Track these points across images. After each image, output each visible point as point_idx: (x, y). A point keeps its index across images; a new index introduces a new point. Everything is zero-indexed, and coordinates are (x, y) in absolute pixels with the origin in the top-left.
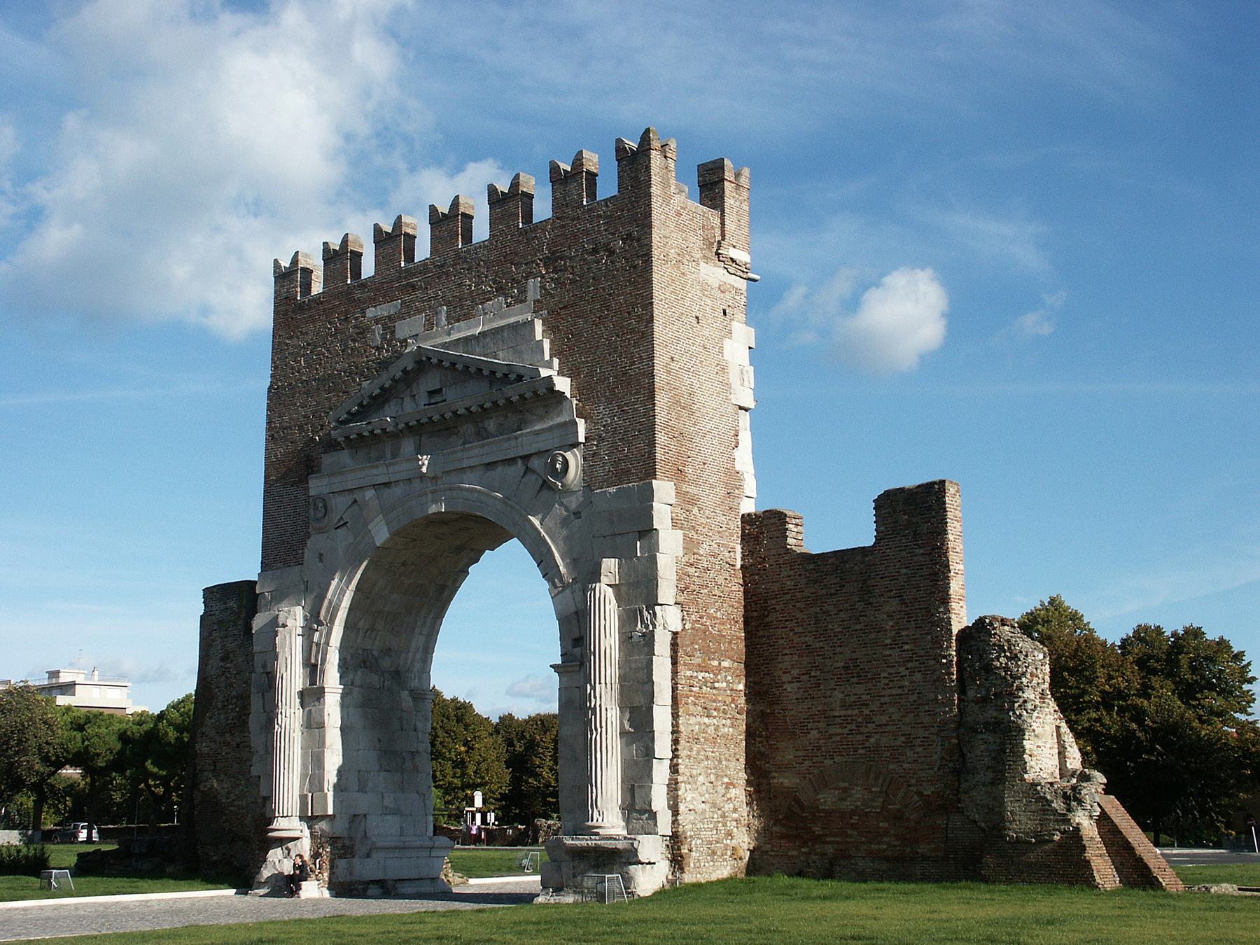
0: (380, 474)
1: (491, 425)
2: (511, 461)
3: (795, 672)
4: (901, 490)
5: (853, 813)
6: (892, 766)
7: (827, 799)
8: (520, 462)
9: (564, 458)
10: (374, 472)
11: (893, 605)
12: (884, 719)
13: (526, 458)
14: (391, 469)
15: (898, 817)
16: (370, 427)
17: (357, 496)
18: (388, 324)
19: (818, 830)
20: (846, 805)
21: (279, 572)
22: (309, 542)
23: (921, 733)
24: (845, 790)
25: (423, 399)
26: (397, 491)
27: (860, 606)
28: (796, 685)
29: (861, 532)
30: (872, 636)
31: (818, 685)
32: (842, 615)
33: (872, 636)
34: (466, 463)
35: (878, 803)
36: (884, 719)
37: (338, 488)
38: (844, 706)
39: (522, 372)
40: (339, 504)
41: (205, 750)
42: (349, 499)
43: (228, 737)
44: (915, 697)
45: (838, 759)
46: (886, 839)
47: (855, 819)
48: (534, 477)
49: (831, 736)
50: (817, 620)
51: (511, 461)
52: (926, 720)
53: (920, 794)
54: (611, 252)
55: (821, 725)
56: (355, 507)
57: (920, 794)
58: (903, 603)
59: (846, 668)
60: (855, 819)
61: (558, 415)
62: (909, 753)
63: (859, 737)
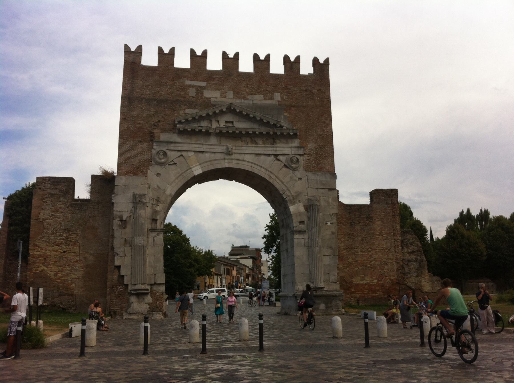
0: (197, 147)
1: (260, 141)
2: (269, 155)
3: (343, 240)
4: (382, 190)
5: (366, 284)
6: (380, 271)
7: (356, 280)
8: (273, 156)
9: (297, 159)
10: (197, 146)
11: (380, 222)
12: (376, 256)
13: (276, 155)
14: (205, 146)
15: (383, 286)
16: (200, 128)
17: (184, 154)
18: (200, 90)
19: (353, 290)
20: (364, 282)
21: (131, 178)
22: (150, 167)
23: (390, 261)
24: (363, 277)
25: (222, 124)
26: (207, 155)
27: (367, 222)
28: (343, 244)
29: (366, 201)
30: (372, 231)
31: (352, 245)
32: (360, 224)
33: (372, 231)
34: (247, 152)
35: (375, 281)
36: (376, 256)
37: (172, 148)
38: (362, 251)
39: (283, 124)
40: (172, 155)
41: (38, 253)
42: (179, 154)
43: (57, 248)
44: (388, 250)
45: (360, 268)
46: (378, 293)
47: (367, 286)
48: (279, 162)
49: (357, 261)
50: (351, 224)
51: (269, 155)
52: (391, 257)
53: (389, 279)
54: (313, 93)
55: (353, 257)
56: (181, 157)
57: (389, 279)
58: (383, 222)
59: (362, 240)
60: (367, 286)
61: (292, 143)
62: (386, 267)
63: (368, 262)
